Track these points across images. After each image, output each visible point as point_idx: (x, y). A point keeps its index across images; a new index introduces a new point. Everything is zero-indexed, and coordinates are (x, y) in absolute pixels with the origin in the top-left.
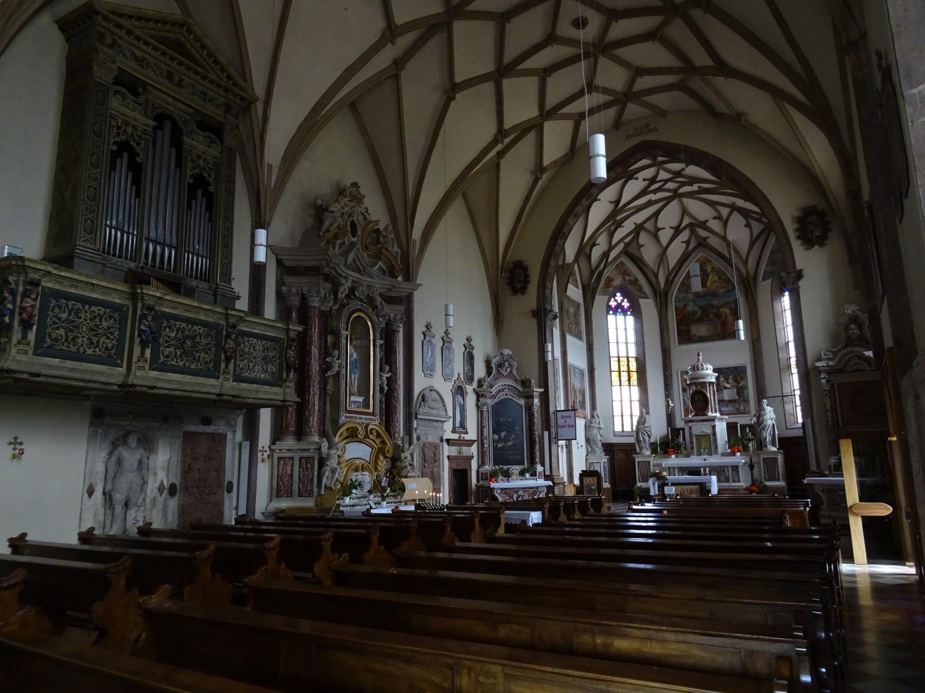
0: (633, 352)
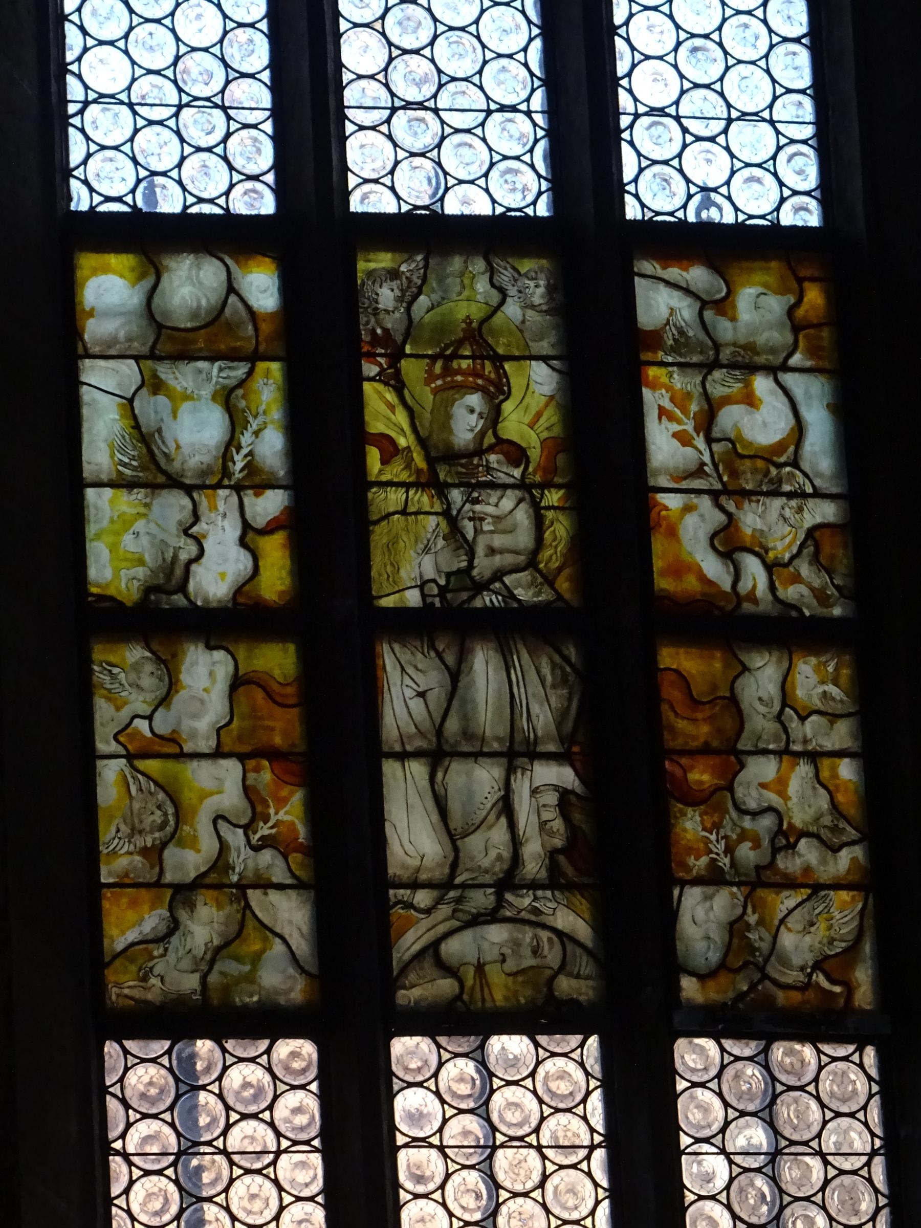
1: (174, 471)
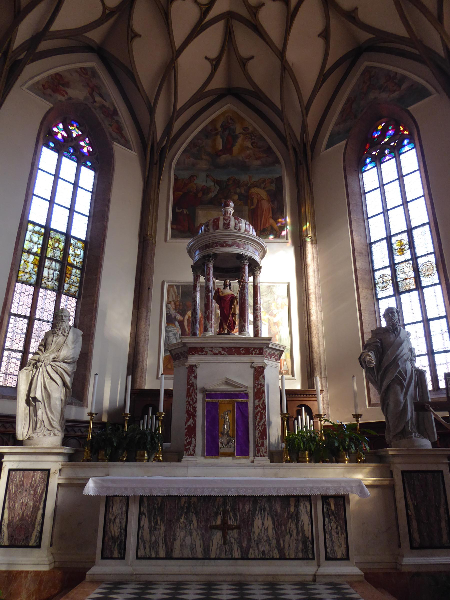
0: (80, 229)
1: (33, 241)
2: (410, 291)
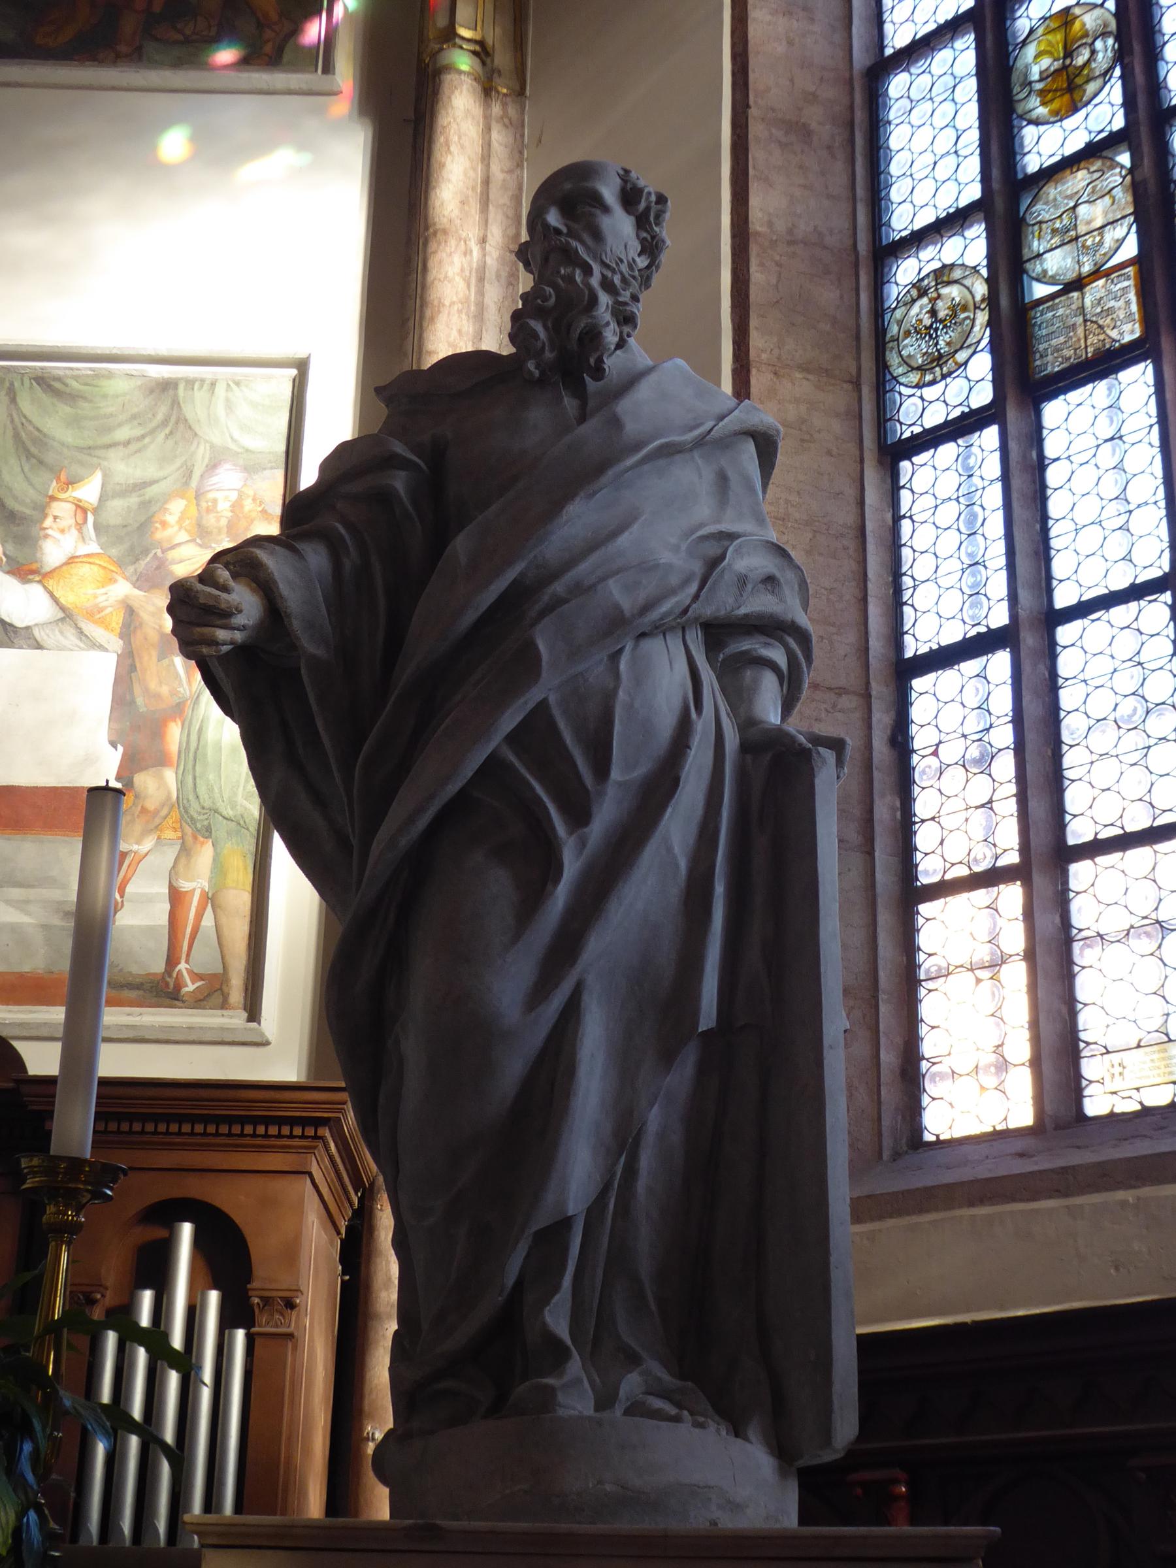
2: (1106, 363)
